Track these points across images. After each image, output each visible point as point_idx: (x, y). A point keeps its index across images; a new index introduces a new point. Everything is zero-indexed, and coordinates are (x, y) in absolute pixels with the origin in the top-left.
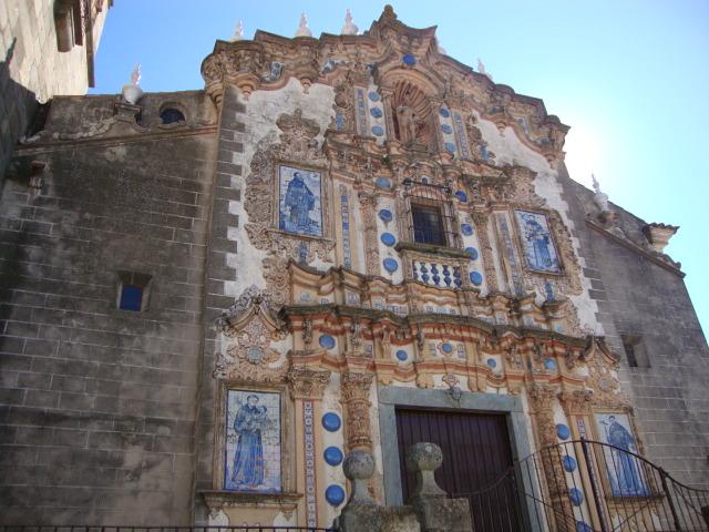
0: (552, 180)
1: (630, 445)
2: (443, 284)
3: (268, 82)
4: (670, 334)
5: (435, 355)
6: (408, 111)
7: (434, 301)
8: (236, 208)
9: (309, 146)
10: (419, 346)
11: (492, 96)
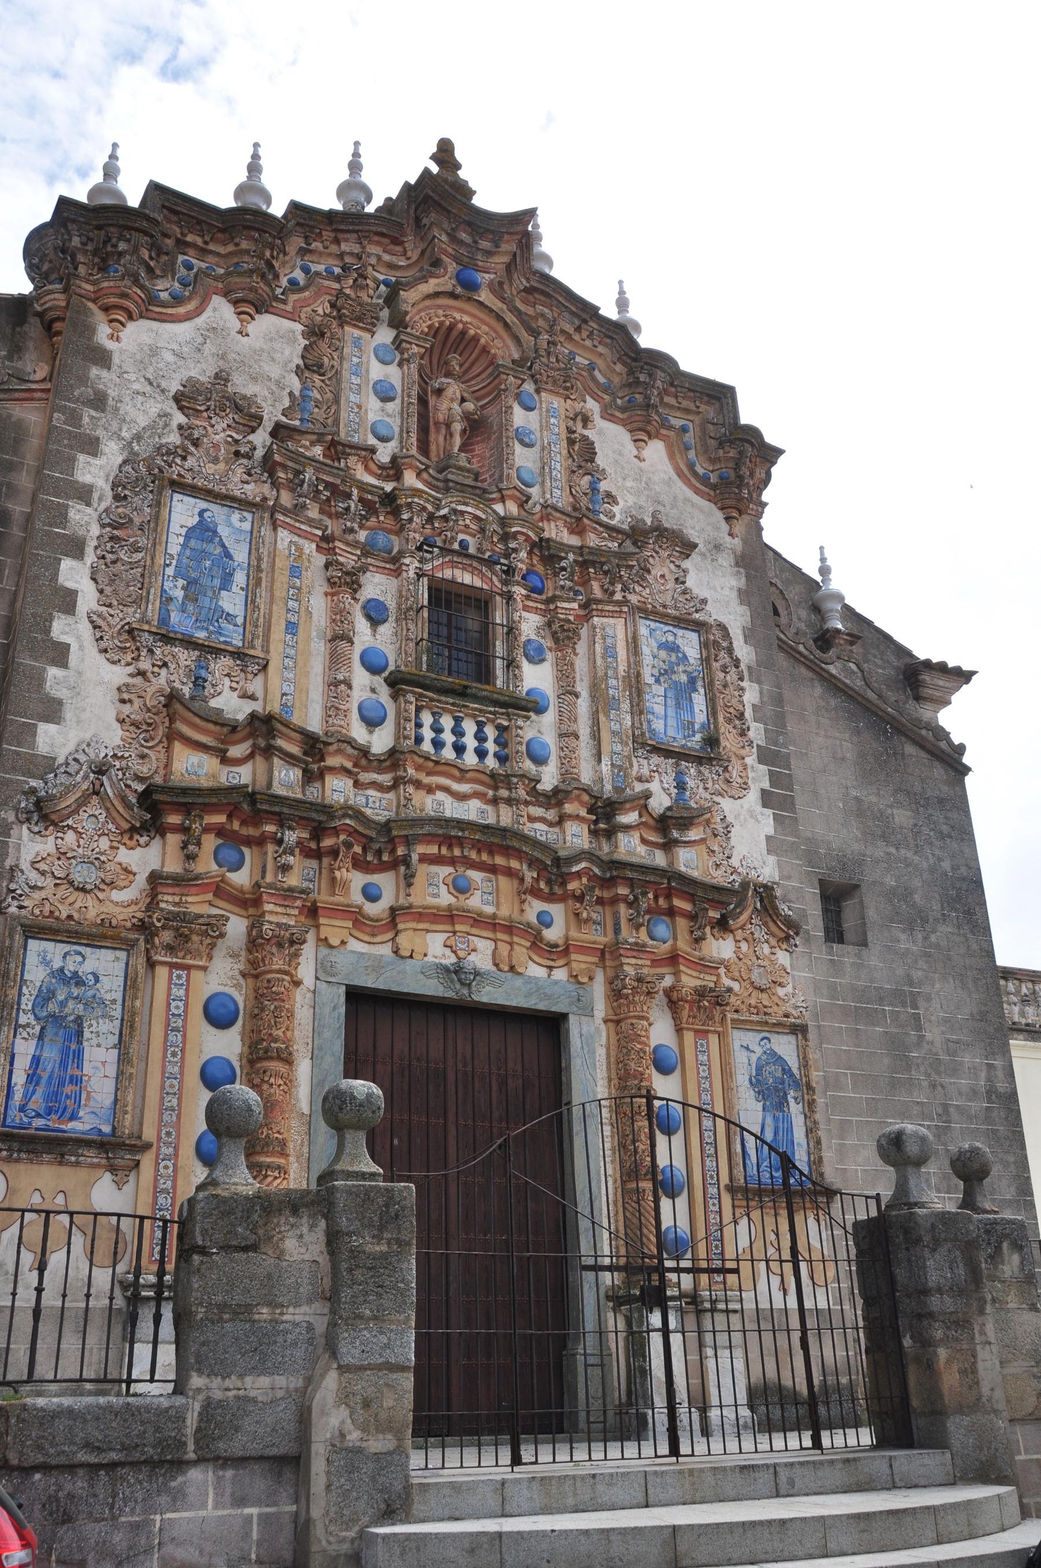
0: (726, 560)
1: (792, 1093)
2: (470, 759)
3: (164, 305)
4: (917, 883)
5: (436, 896)
6: (454, 389)
7: (447, 790)
8: (74, 574)
9: (237, 454)
10: (406, 877)
11: (631, 372)
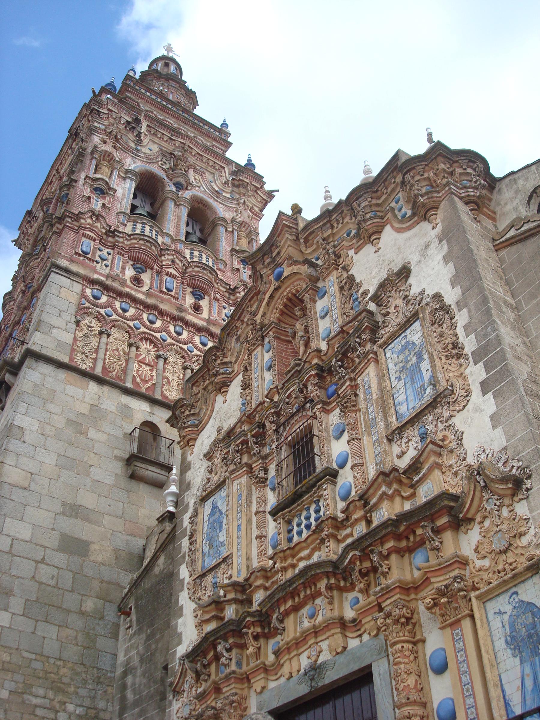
7: (302, 559)
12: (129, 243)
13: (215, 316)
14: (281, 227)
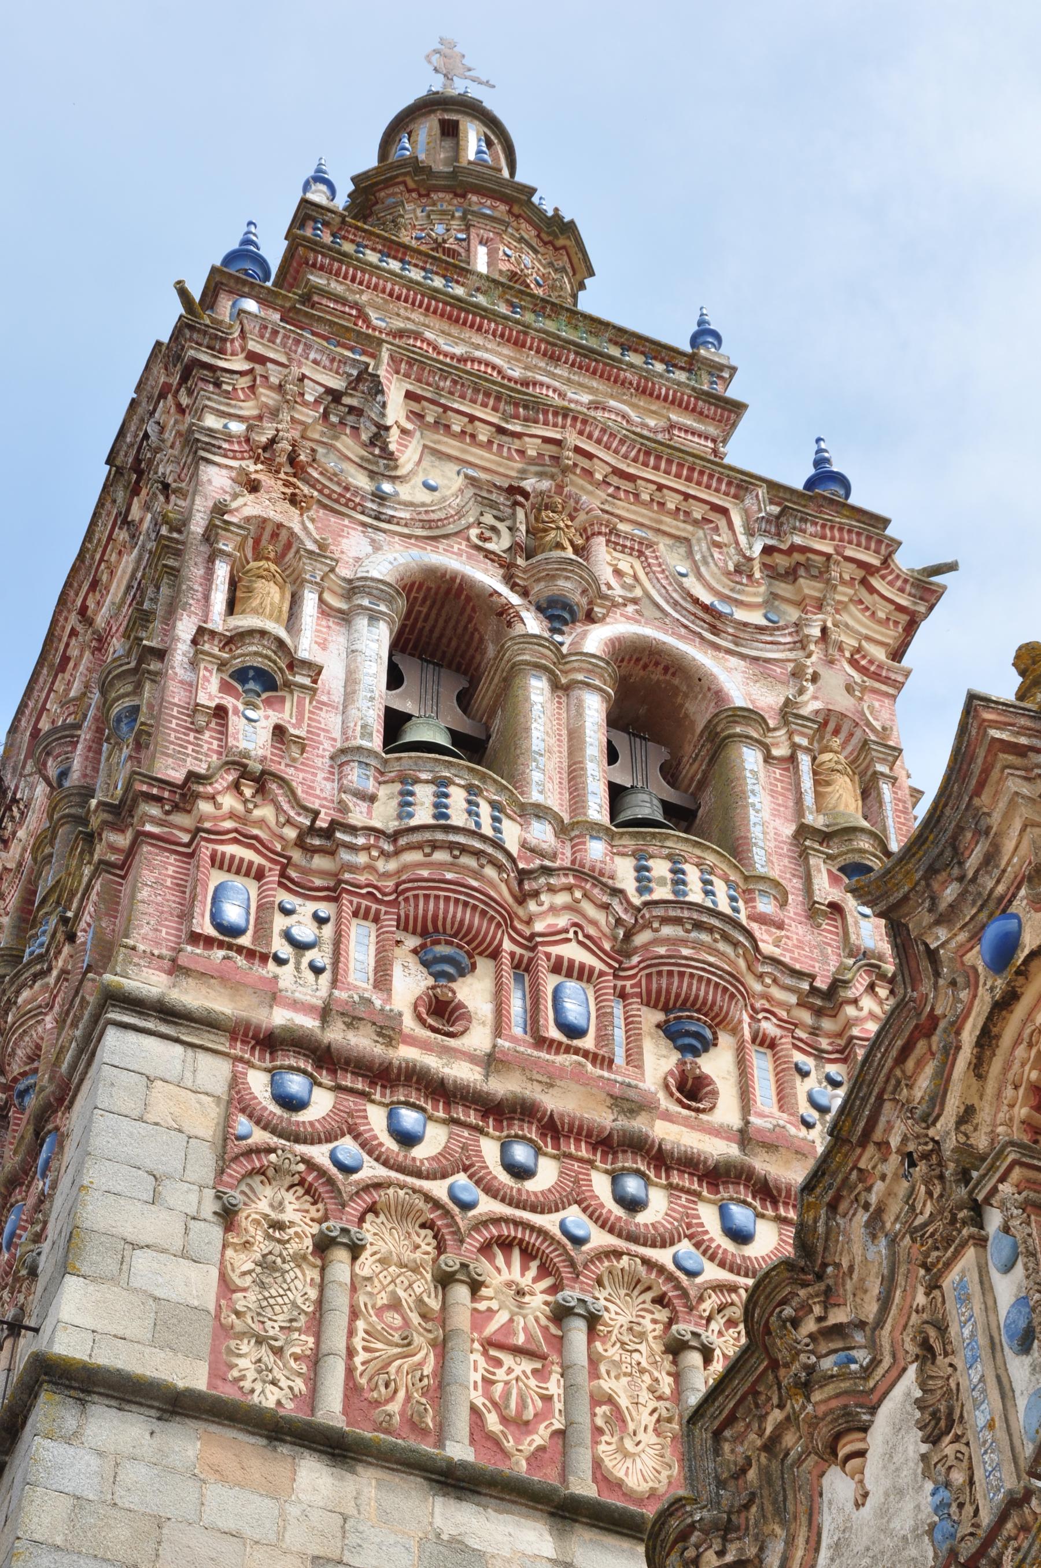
12: (392, 866)
13: (767, 1113)
14: (981, 753)
